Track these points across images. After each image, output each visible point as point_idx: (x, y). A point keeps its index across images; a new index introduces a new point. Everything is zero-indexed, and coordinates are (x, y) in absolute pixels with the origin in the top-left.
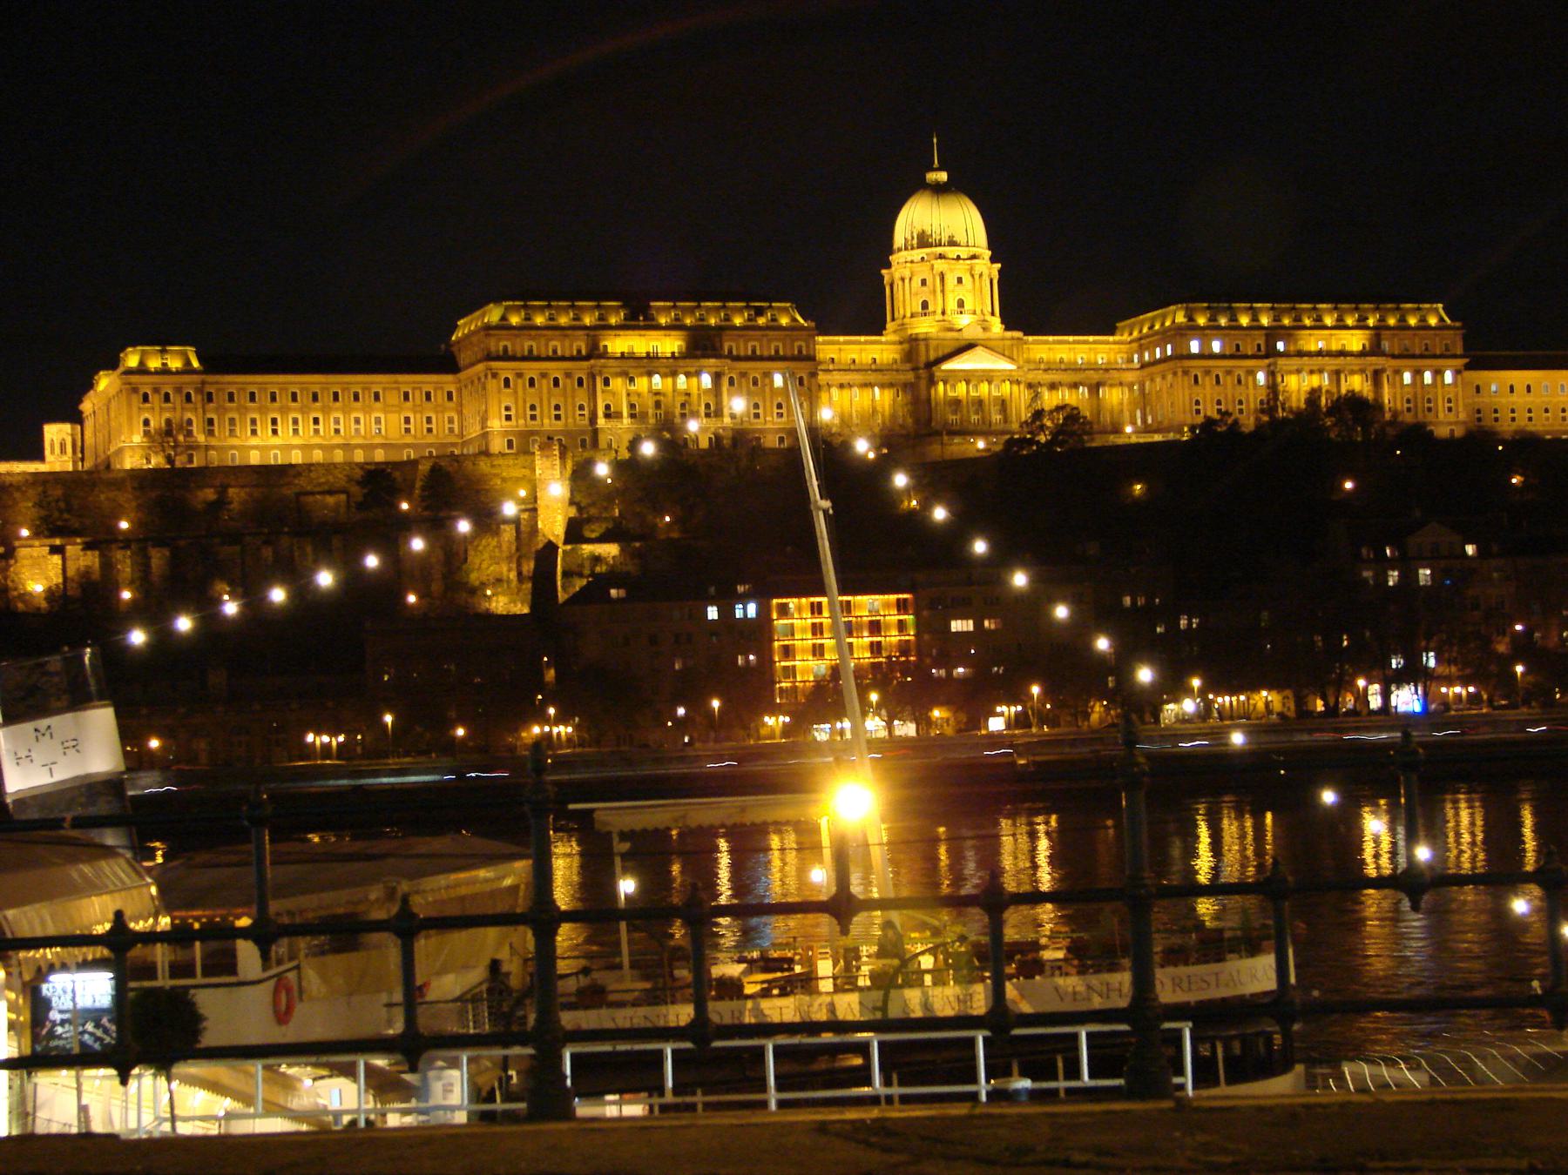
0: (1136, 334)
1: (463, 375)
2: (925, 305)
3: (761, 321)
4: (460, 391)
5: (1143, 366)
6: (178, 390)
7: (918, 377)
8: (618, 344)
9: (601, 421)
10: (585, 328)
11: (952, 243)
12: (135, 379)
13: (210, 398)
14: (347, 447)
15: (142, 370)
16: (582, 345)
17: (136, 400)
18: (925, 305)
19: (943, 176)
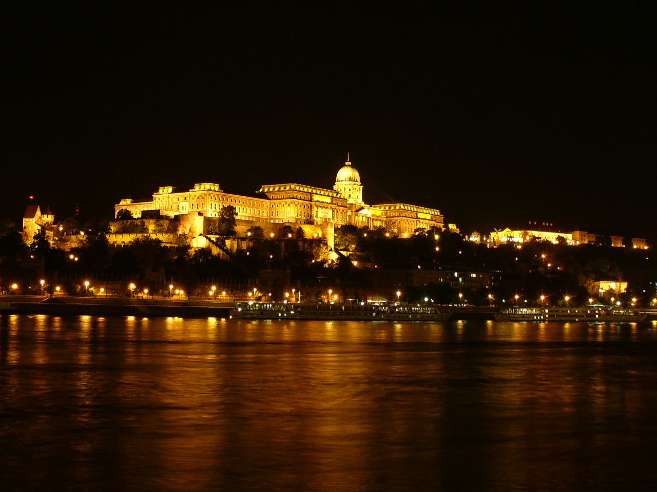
0: (382, 208)
1: (272, 201)
2: (350, 196)
3: (338, 196)
4: (270, 205)
5: (387, 217)
6: (218, 197)
7: (352, 214)
8: (316, 198)
9: (315, 218)
10: (311, 193)
11: (357, 181)
12: (211, 192)
13: (223, 200)
14: (249, 217)
15: (210, 190)
16: (308, 197)
17: (210, 198)
18: (350, 196)
19: (350, 163)
